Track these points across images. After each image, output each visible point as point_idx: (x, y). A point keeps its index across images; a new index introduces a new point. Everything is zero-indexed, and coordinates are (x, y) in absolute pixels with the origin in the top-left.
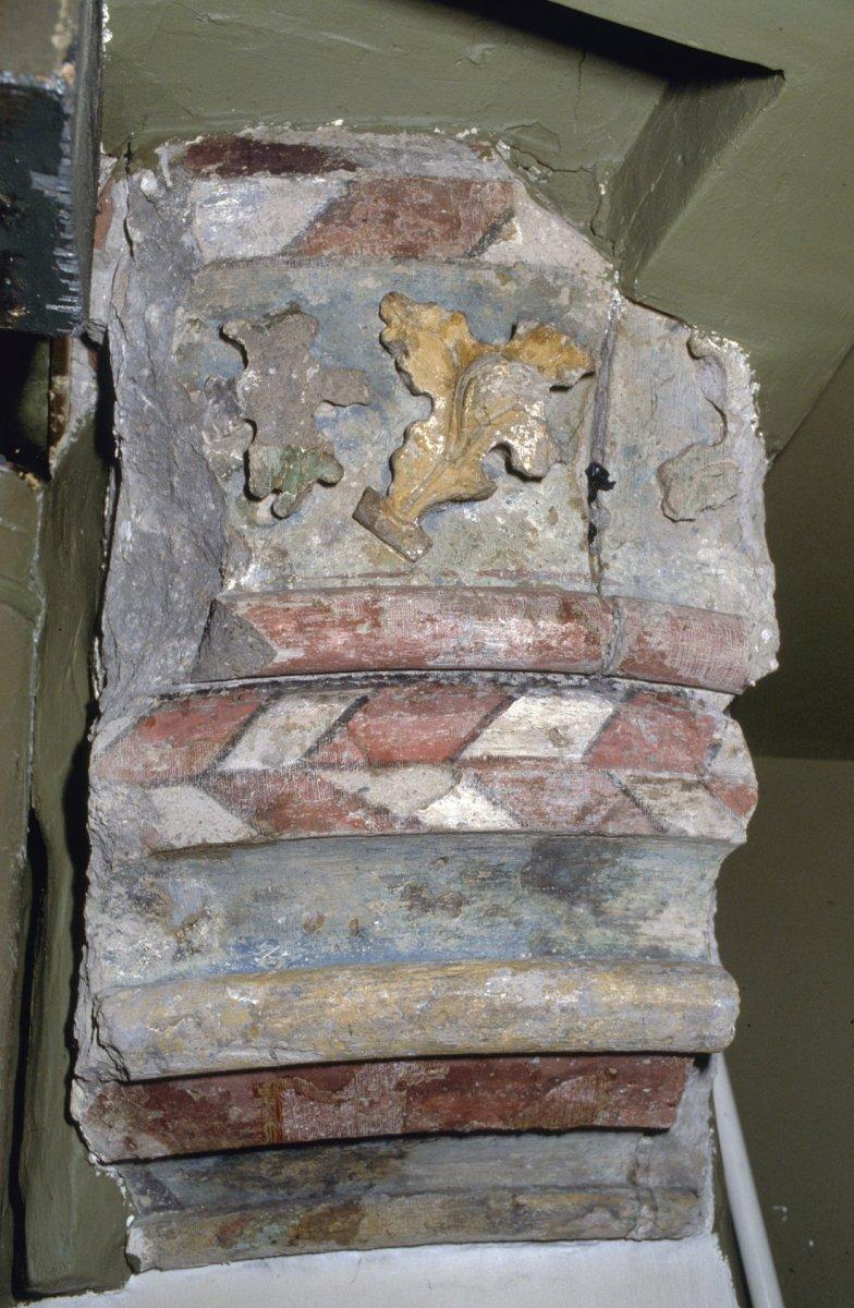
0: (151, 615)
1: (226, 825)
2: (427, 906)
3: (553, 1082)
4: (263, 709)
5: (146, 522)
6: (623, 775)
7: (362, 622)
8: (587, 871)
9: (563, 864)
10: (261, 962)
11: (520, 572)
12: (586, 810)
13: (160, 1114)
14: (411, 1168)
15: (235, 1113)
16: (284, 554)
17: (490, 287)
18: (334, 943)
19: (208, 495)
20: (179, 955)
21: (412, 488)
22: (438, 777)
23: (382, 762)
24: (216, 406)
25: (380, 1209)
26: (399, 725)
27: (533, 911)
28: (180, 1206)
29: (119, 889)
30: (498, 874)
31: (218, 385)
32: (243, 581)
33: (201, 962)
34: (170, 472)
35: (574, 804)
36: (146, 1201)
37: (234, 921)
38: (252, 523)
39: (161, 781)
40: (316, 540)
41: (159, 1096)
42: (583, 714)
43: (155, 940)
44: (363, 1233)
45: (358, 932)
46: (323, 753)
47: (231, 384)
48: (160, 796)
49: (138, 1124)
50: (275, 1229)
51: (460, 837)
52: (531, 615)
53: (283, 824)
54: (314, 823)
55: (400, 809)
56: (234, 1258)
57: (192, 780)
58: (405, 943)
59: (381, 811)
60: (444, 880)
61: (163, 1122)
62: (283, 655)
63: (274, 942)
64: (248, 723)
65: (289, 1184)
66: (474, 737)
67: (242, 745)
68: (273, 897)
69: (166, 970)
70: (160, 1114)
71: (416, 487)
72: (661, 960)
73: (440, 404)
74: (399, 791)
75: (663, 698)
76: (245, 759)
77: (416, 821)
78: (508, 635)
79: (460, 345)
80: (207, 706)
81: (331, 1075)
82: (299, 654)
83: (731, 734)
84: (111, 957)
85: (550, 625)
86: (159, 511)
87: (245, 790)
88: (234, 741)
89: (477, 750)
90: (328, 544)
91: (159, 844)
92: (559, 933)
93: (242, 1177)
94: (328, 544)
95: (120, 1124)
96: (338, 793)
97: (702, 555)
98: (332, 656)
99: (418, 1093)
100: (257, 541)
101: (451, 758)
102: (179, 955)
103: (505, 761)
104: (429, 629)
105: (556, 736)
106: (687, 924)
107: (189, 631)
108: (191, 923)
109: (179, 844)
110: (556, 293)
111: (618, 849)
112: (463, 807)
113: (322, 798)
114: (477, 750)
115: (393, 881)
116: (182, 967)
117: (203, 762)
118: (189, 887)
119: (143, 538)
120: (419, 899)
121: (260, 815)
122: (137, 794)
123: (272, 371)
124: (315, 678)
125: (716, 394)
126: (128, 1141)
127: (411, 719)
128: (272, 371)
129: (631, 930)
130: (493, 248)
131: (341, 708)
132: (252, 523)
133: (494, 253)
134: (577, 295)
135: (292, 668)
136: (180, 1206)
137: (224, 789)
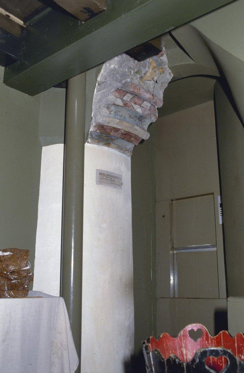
0: (114, 77)
1: (121, 104)
2: (130, 118)
3: (132, 137)
4: (126, 94)
5: (116, 67)
6: (151, 112)
8: (142, 119)
9: (141, 118)
10: (116, 117)
11: (148, 89)
12: (147, 114)
13: (101, 128)
14: (115, 141)
15: (107, 131)
17: (158, 60)
18: (122, 118)
19: (127, 69)
20: (109, 114)
21: (145, 78)
22: (139, 107)
23: (135, 104)
25: (112, 145)
26: (137, 100)
27: (137, 121)
28: (93, 138)
29: (107, 105)
30: (137, 116)
32: (128, 80)
33: (111, 115)
34: (123, 64)
35: (147, 113)
36: (90, 136)
37: (115, 112)
38: (131, 74)
39: (118, 98)
40: (135, 79)
41: (101, 127)
42: (149, 105)
43: (108, 112)
44: (110, 146)
45: (125, 118)
46: (131, 101)
48: (118, 99)
49: (98, 129)
50: (103, 143)
51: (137, 112)
52: (150, 95)
53: (126, 106)
54: (128, 107)
55: (135, 108)
56: (98, 145)
57: (121, 99)
58: (128, 120)
59: (134, 108)
60: (132, 115)
61: (100, 129)
62: (131, 90)
63: (118, 116)
64: (125, 95)
65: (104, 139)
66: (142, 104)
67: (125, 97)
68: (118, 111)
69: (108, 115)
70: (101, 128)
71: (146, 78)
72: (144, 129)
73: (150, 70)
74: (136, 107)
75: (154, 106)
76: (125, 98)
77: (135, 110)
78: (148, 96)
79: (154, 65)
80: (121, 91)
81: (117, 130)
82: (132, 90)
83: (157, 111)
84: (103, 112)
85: (151, 96)
86: (118, 66)
87: (124, 101)
88: (124, 96)
89: (142, 105)
90: (136, 79)
91: (115, 103)
92: (138, 124)
93: (100, 137)
94: (136, 79)
95: (97, 128)
96: (131, 105)
97: (160, 93)
98: (135, 92)
99: (123, 134)
101: (140, 105)
102: (109, 114)
103: (143, 107)
104: (143, 93)
105: (147, 106)
106: (146, 127)
107: (120, 82)
108: (111, 111)
109: (117, 104)
110: (163, 63)
111: (146, 118)
112: (139, 110)
113: (130, 105)
114: (142, 105)
115: (129, 114)
116: (110, 115)
117: (121, 97)
118: (113, 108)
119: (114, 67)
120: (130, 116)
121: (125, 104)
122: (116, 98)
124: (131, 93)
126: (96, 130)
127: (137, 100)
129: (143, 126)
130: (161, 57)
131: (133, 97)
132: (131, 74)
133: (161, 58)
134: (164, 64)
135: (131, 91)
136: (93, 138)
137: (123, 100)
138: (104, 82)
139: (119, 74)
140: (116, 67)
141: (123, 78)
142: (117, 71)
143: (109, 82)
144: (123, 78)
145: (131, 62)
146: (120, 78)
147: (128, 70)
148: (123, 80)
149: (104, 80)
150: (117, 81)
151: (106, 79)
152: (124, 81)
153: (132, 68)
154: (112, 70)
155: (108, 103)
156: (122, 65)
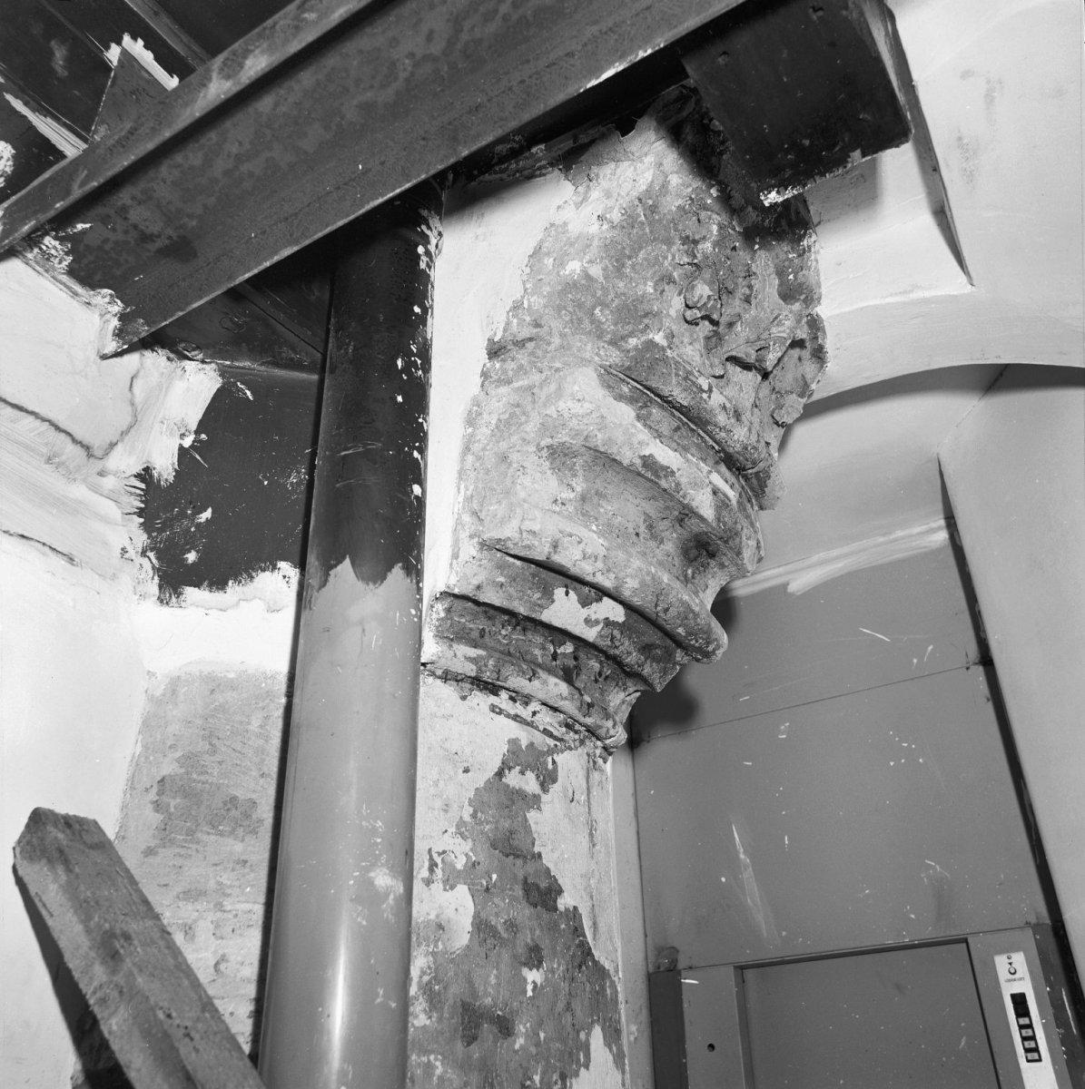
0: (580, 321)
7: (705, 392)
16: (673, 336)
24: (682, 247)
31: (688, 237)
34: (630, 258)
47: (696, 242)
61: (502, 585)
86: (604, 269)
100: (667, 322)
107: (613, 343)
123: (717, 250)
125: (808, 377)
126: (478, 587)
128: (717, 250)
138: (531, 339)
139: (604, 305)
140: (596, 271)
141: (630, 328)
142: (599, 293)
143: (556, 341)
144: (630, 328)
145: (674, 248)
146: (616, 325)
147: (655, 290)
148: (631, 334)
149: (526, 332)
150: (600, 337)
151: (537, 325)
152: (633, 342)
153: (674, 282)
154: (570, 286)
155: (555, 442)
156: (623, 265)
